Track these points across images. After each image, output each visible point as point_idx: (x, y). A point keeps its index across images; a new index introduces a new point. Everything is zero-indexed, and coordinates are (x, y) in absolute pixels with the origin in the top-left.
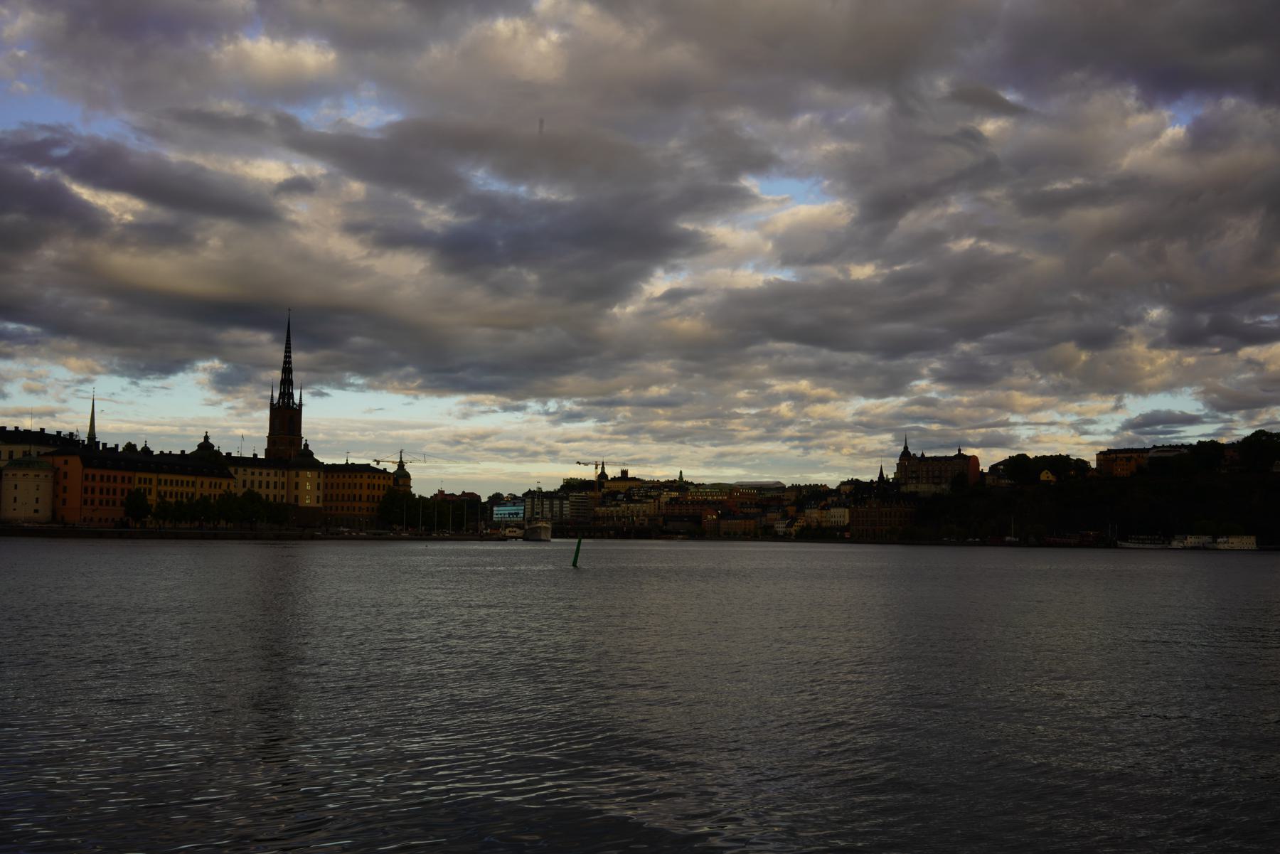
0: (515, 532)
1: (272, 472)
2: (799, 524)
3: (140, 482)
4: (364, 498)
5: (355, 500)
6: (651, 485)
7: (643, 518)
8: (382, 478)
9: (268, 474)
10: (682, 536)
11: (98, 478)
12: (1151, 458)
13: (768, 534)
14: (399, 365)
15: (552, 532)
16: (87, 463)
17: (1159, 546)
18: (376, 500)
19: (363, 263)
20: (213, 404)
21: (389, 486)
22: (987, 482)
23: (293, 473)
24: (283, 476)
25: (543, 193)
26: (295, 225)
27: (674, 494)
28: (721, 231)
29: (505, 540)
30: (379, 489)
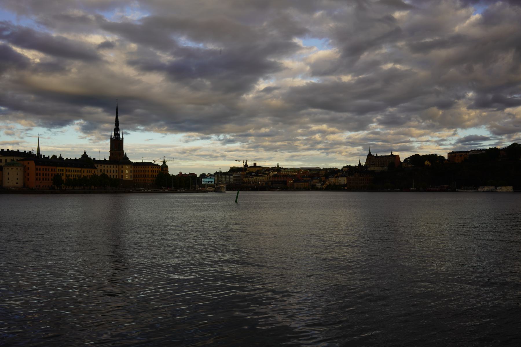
0: (211, 189)
1: (112, 166)
4: (150, 176)
6: (266, 169)
7: (263, 182)
8: (157, 168)
9: (110, 167)
10: (279, 190)
11: (42, 170)
12: (470, 155)
13: (313, 188)
14: (157, 121)
15: (226, 188)
16: (37, 163)
17: (473, 191)
18: (154, 177)
19: (138, 78)
20: (83, 138)
21: (160, 171)
22: (403, 166)
23: (121, 166)
24: (117, 167)
25: (211, 46)
26: (107, 62)
27: (275, 173)
28: (288, 62)
29: (207, 192)
30: (155, 172)
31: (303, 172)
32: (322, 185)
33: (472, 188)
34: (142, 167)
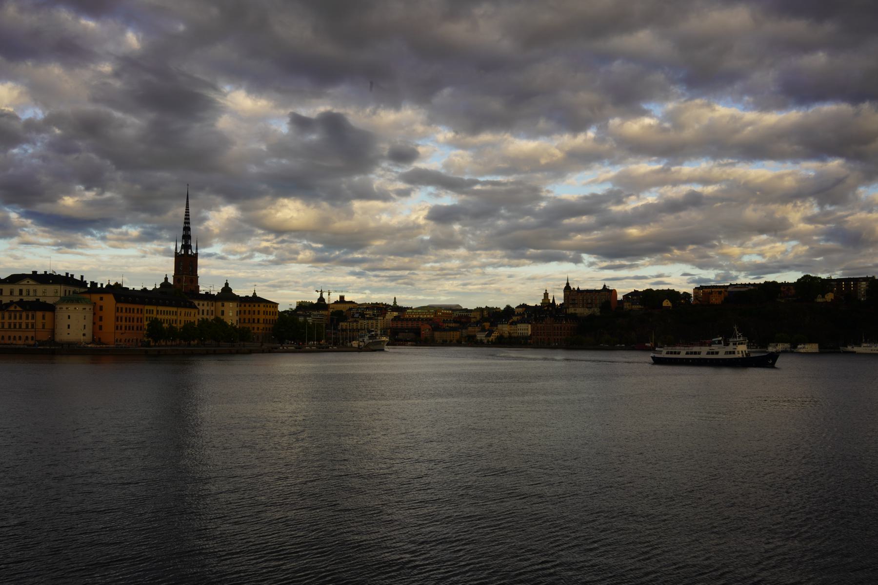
1: (206, 303)
2: (495, 335)
3: (147, 313)
4: (261, 321)
5: (254, 322)
6: (365, 307)
8: (272, 307)
9: (203, 305)
10: (410, 343)
12: (730, 292)
13: (471, 342)
16: (118, 299)
22: (625, 307)
23: (220, 304)
27: (396, 314)
30: (270, 314)
31: (443, 313)
32: (489, 335)
33: (753, 345)
34: (206, 305)
